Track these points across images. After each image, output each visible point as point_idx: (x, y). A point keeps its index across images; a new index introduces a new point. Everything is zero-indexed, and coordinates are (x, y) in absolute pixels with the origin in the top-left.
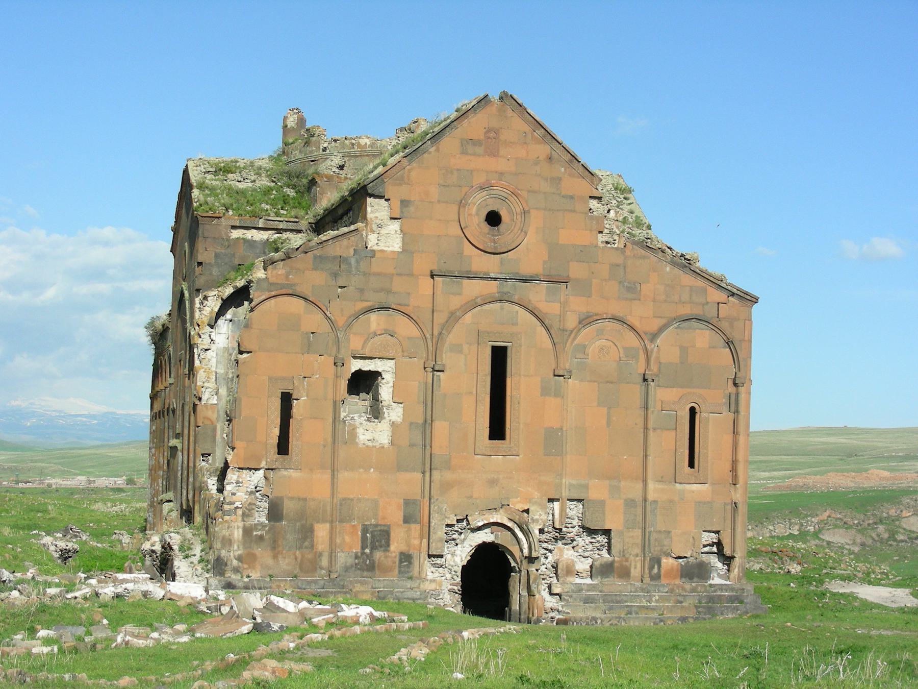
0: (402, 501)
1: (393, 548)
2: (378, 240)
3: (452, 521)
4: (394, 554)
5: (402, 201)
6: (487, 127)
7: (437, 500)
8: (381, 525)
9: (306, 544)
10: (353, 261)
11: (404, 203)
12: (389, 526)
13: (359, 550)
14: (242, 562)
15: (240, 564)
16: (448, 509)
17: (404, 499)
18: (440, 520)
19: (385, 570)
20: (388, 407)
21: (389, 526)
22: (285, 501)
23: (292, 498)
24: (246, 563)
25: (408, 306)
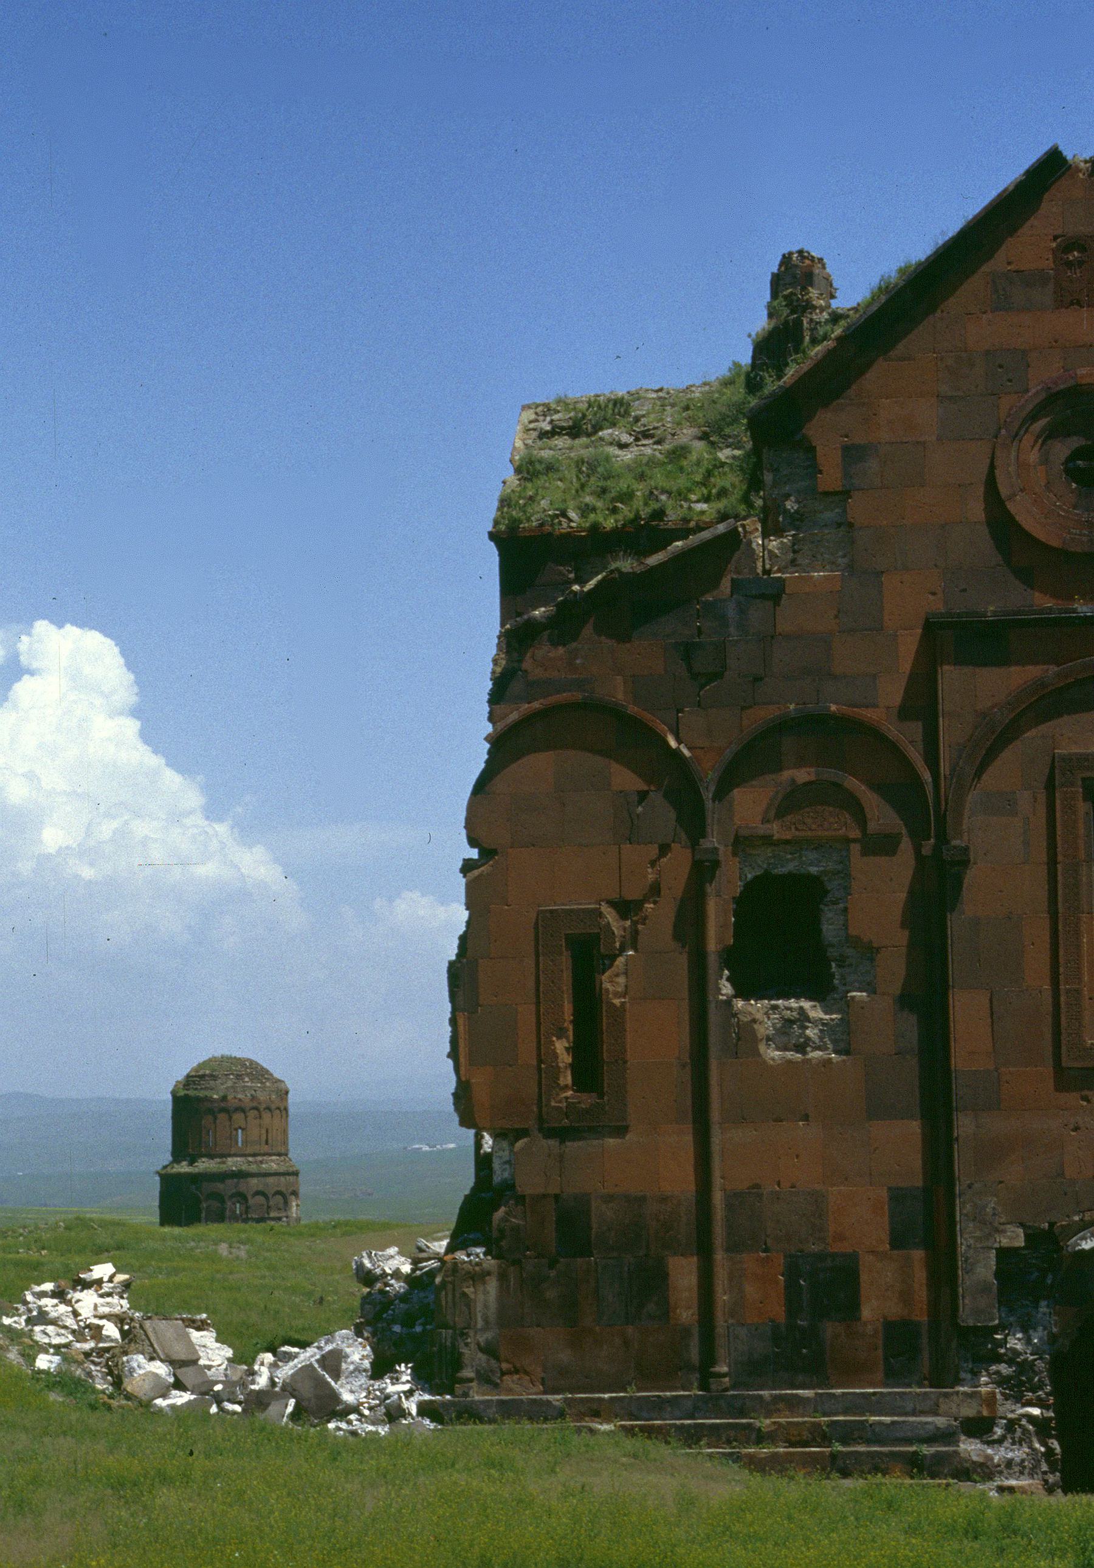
0: (884, 1193)
1: (866, 1313)
2: (794, 552)
3: (1011, 1238)
4: (869, 1329)
5: (846, 449)
6: (1059, 232)
7: (970, 1186)
8: (834, 1256)
9: (651, 1307)
10: (731, 612)
11: (853, 454)
12: (853, 1258)
13: (782, 1319)
14: (498, 1359)
15: (493, 1362)
16: (1000, 1209)
17: (889, 1189)
18: (978, 1239)
19: (853, 1372)
20: (842, 962)
21: (853, 1258)
22: (594, 1204)
23: (609, 1198)
24: (507, 1361)
25: (875, 706)
